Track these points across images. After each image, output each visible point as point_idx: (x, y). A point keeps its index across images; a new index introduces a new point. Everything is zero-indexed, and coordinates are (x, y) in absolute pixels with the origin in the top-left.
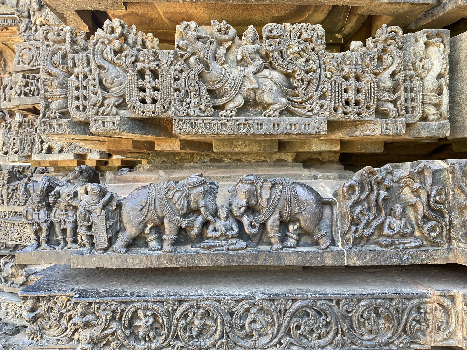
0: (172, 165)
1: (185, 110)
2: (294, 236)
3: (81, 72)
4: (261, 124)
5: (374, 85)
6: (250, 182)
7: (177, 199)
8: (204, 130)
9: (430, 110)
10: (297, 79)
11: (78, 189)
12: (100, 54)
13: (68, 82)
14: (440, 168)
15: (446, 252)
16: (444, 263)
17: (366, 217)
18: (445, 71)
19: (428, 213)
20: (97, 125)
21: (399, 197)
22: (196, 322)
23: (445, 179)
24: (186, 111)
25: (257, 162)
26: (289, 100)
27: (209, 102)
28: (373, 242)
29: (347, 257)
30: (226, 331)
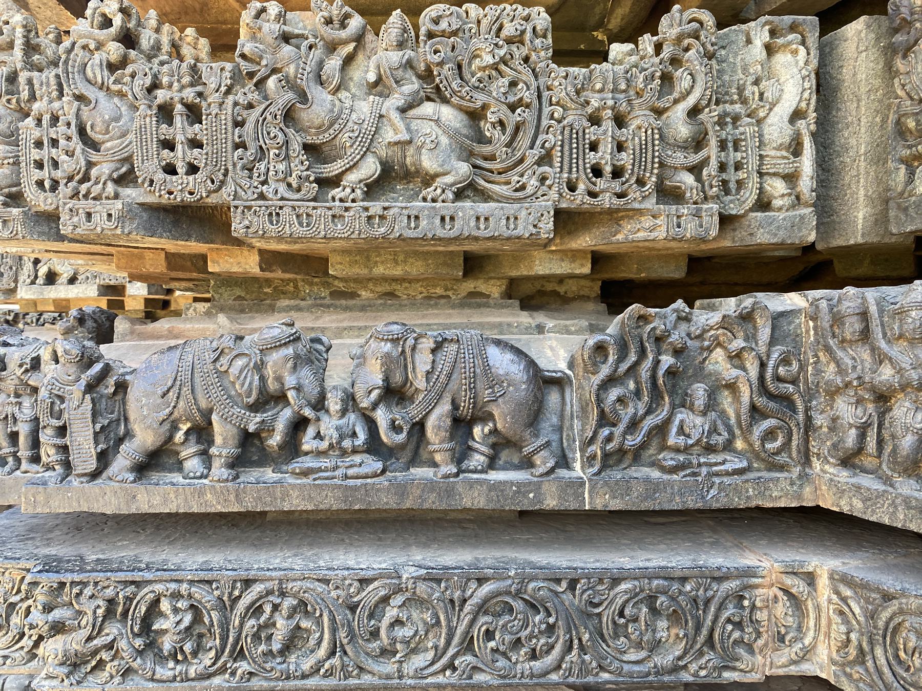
0: (254, 304)
1: (256, 187)
2: (483, 449)
3: (45, 109)
4: (417, 217)
5: (653, 133)
6: (390, 337)
7: (237, 372)
8: (297, 228)
10: (492, 123)
11: (41, 352)
12: (79, 72)
13: (21, 132)
14: (789, 308)
16: (793, 505)
17: (631, 410)
18: (808, 104)
19: (761, 402)
20: (75, 219)
21: (702, 369)
22: (280, 622)
23: (799, 331)
24: (259, 190)
25: (429, 298)
26: (475, 166)
27: (307, 170)
28: (648, 460)
29: (590, 492)
30: (341, 641)
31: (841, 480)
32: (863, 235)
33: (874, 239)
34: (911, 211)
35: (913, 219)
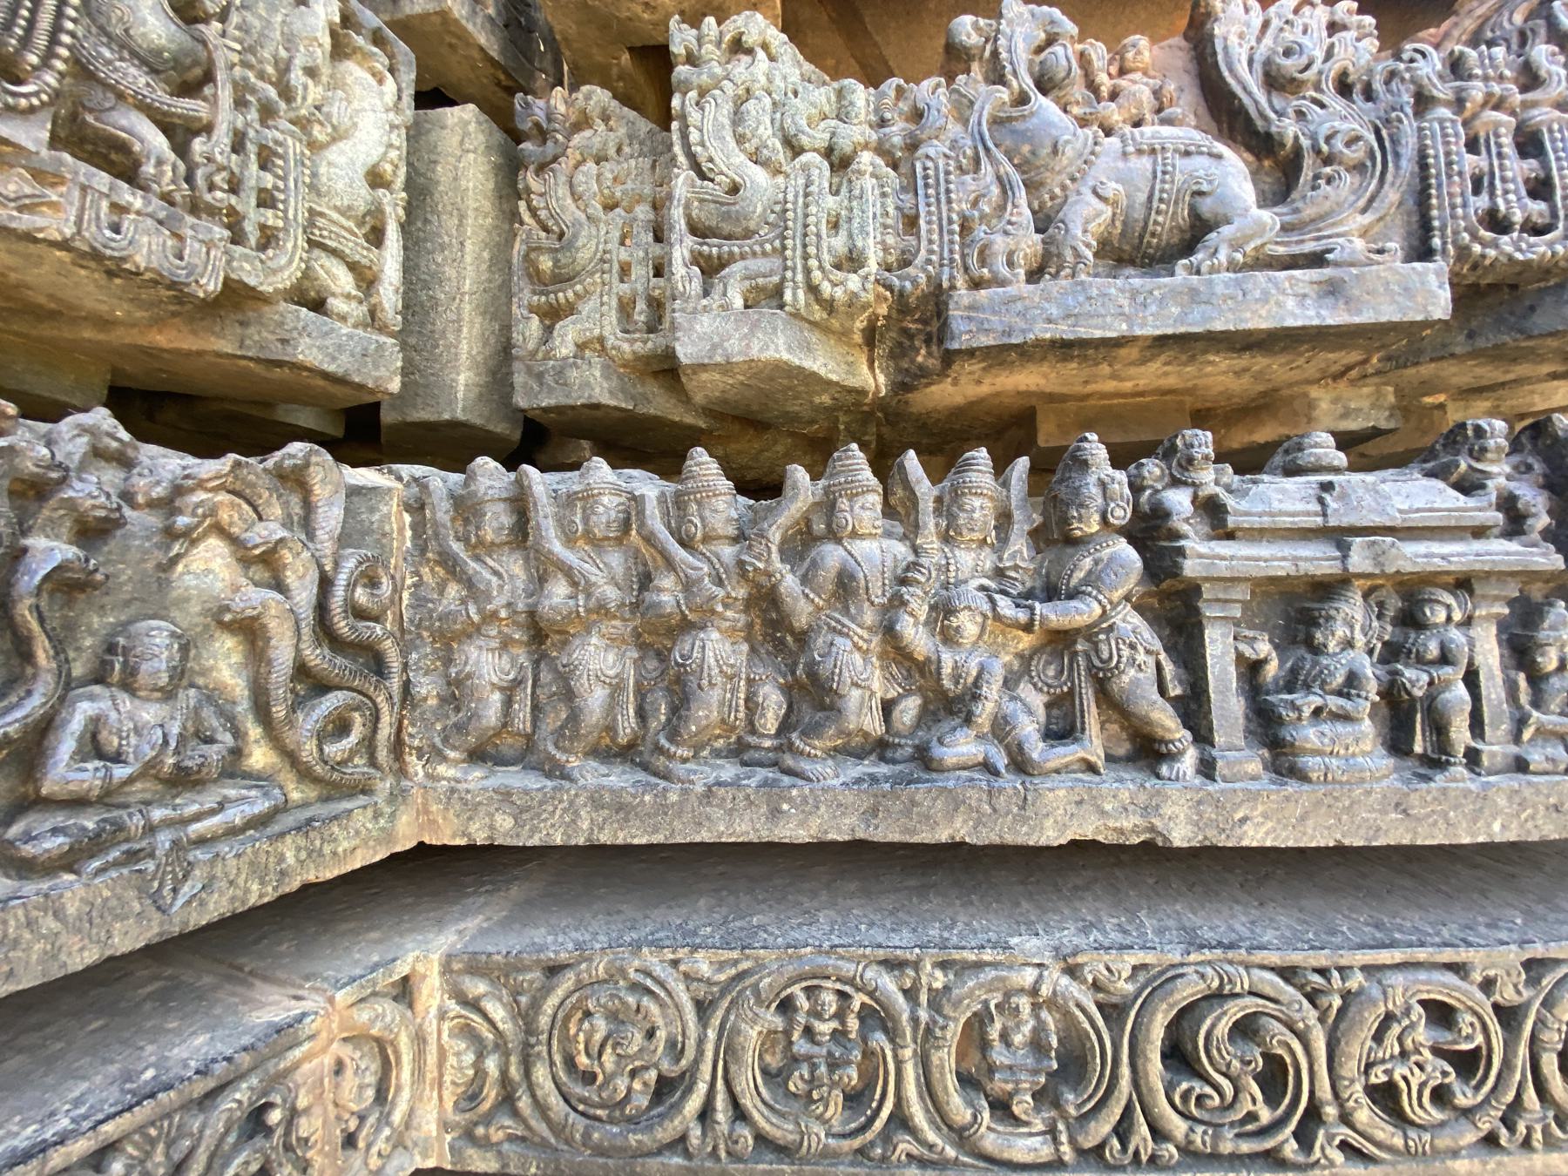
9: (334, 278)
15: (388, 810)
16: (377, 858)
19: (316, 656)
23: (387, 528)
31: (471, 786)
32: (464, 409)
34: (549, 379)
35: (551, 390)
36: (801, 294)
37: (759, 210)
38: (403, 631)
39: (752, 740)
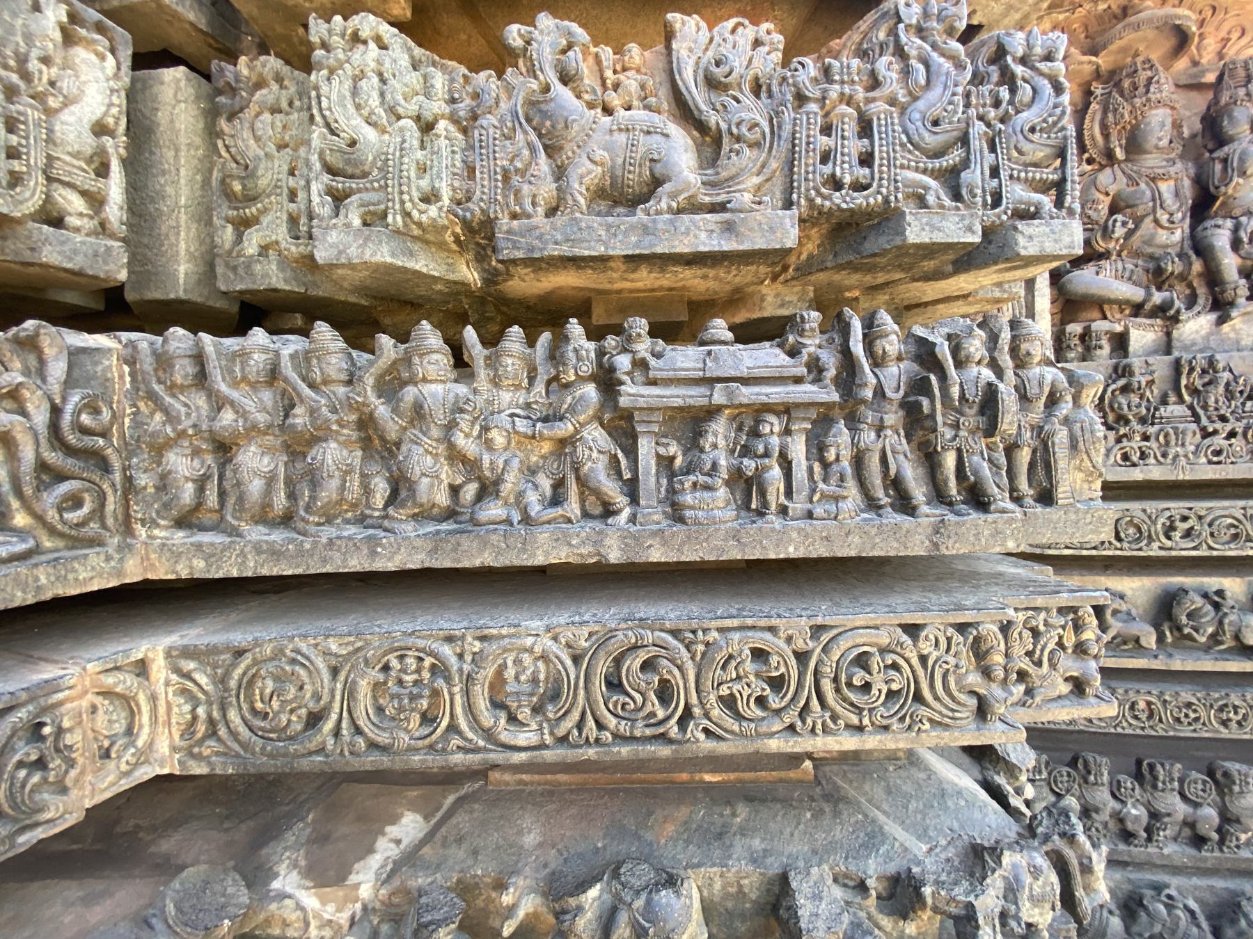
15: (117, 556)
16: (111, 585)
19: (53, 457)
23: (109, 375)
32: (185, 290)
33: (196, 297)
34: (241, 271)
35: (242, 279)
36: (399, 218)
37: (370, 158)
38: (126, 444)
39: (368, 512)
